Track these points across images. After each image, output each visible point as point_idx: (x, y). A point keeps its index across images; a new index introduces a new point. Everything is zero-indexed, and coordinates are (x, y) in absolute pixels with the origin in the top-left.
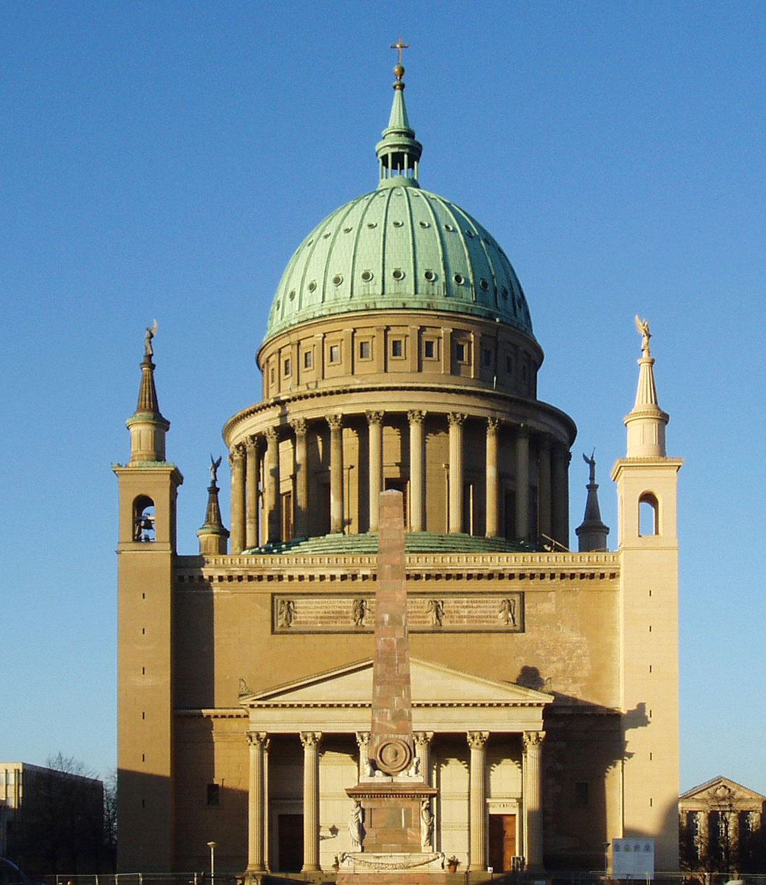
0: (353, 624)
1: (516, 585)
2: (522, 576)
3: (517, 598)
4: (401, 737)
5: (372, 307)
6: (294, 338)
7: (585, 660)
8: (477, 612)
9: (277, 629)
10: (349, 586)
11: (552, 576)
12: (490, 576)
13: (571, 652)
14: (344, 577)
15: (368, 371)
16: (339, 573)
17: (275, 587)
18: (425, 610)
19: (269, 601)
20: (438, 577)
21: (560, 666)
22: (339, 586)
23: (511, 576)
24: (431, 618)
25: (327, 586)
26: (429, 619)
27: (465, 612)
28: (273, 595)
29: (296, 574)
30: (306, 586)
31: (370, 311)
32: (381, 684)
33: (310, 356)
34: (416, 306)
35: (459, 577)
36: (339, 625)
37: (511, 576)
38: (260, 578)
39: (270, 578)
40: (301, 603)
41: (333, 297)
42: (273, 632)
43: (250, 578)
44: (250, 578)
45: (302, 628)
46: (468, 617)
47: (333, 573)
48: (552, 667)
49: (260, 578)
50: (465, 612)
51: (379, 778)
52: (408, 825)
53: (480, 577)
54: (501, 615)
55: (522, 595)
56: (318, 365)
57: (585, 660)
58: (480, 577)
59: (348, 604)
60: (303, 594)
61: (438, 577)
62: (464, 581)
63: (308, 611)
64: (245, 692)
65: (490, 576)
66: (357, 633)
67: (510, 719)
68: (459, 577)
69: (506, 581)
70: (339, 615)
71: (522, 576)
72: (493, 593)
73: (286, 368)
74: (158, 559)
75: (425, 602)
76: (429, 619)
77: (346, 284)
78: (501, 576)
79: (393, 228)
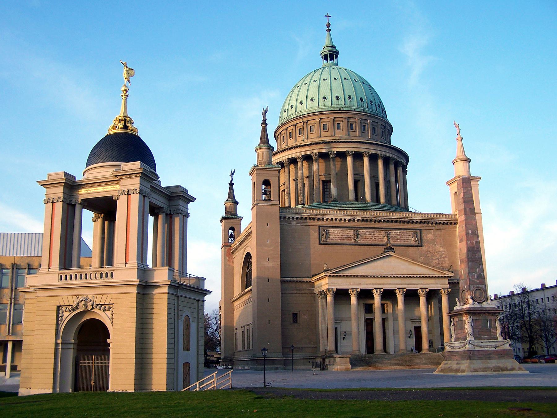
0: (353, 241)
1: (418, 226)
2: (421, 223)
3: (418, 231)
6: (305, 120)
8: (403, 237)
9: (322, 242)
10: (351, 224)
11: (432, 223)
12: (408, 222)
13: (441, 256)
14: (350, 220)
15: (341, 134)
16: (348, 218)
17: (320, 223)
19: (317, 229)
20: (388, 221)
21: (437, 261)
22: (347, 224)
23: (417, 222)
24: (386, 239)
25: (342, 224)
26: (385, 240)
27: (398, 237)
28: (320, 227)
29: (330, 218)
31: (341, 111)
33: (313, 128)
34: (359, 110)
35: (396, 222)
36: (347, 241)
37: (417, 222)
38: (314, 219)
39: (319, 219)
40: (331, 231)
42: (320, 244)
43: (310, 219)
44: (310, 219)
45: (332, 242)
46: (400, 239)
49: (314, 219)
50: (398, 237)
51: (477, 305)
52: (491, 327)
53: (404, 222)
54: (413, 239)
55: (420, 230)
56: (317, 131)
57: (446, 259)
58: (404, 222)
59: (351, 231)
60: (332, 227)
62: (398, 224)
63: (335, 234)
65: (408, 222)
66: (355, 245)
68: (396, 222)
69: (414, 224)
70: (347, 237)
71: (421, 223)
72: (410, 229)
74: (274, 209)
75: (382, 232)
76: (385, 240)
78: (413, 222)
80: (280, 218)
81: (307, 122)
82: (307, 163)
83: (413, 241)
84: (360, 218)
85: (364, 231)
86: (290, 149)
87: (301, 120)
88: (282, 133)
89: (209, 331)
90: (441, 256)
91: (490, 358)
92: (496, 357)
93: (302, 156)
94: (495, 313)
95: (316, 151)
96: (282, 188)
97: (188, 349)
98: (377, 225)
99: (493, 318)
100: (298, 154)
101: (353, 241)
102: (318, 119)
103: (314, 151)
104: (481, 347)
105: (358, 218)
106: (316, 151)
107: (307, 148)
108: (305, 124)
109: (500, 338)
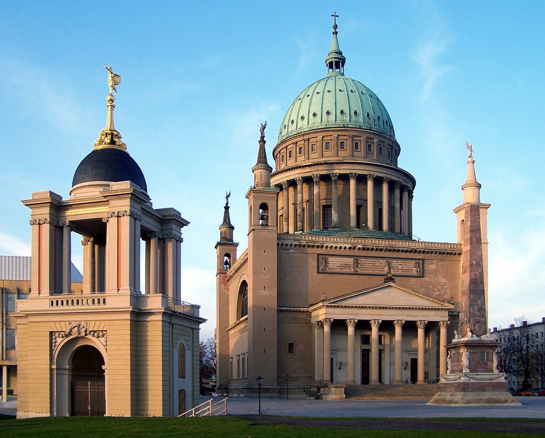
0: (353, 270)
1: (421, 256)
2: (424, 252)
3: (421, 261)
4: (481, 319)
5: (346, 126)
6: (306, 137)
7: (448, 291)
8: (405, 267)
9: (320, 271)
10: (352, 253)
11: (436, 253)
12: (411, 251)
13: (442, 287)
14: (350, 248)
15: (344, 154)
16: (348, 246)
17: (319, 251)
18: (383, 265)
19: (316, 258)
20: (390, 250)
21: (438, 293)
22: (347, 252)
23: (420, 252)
24: (386, 268)
25: (342, 252)
26: (385, 269)
27: (400, 267)
28: (318, 254)
29: (329, 245)
30: (333, 252)
31: (345, 128)
32: (473, 294)
33: (315, 146)
35: (399, 251)
36: (347, 270)
37: (420, 252)
38: (313, 246)
39: (318, 246)
40: (331, 259)
41: (326, 120)
42: (318, 272)
43: (309, 246)
44: (309, 246)
45: (331, 271)
46: (401, 269)
47: (346, 246)
48: (435, 293)
49: (313, 246)
50: (400, 267)
51: (475, 338)
52: (488, 360)
53: (407, 251)
54: (415, 269)
55: (423, 260)
56: (319, 151)
57: (448, 291)
58: (407, 251)
59: (351, 260)
60: (332, 255)
61: (390, 250)
62: (400, 253)
63: (334, 263)
64: (325, 299)
65: (411, 251)
67: (435, 315)
68: (399, 251)
69: (417, 254)
70: (347, 266)
71: (424, 252)
72: (412, 259)
73: (300, 151)
74: (271, 235)
75: (383, 261)
76: (385, 269)
77: (319, 116)
78: (416, 252)
79: (339, 92)
80: (278, 244)
81: (308, 140)
82: (307, 186)
83: (414, 273)
84: (361, 246)
85: (365, 260)
86: (289, 170)
87: (302, 138)
88: (281, 152)
89: (205, 359)
90: (442, 287)
91: (484, 390)
92: (491, 389)
93: (302, 177)
94: (493, 346)
95: (317, 173)
96: (280, 213)
97: (183, 377)
98: (378, 254)
99: (490, 351)
100: (298, 176)
101: (353, 270)
102: (320, 136)
103: (315, 173)
104: (476, 379)
105: (359, 246)
106: (317, 173)
107: (308, 169)
108: (307, 142)
109: (496, 371)
